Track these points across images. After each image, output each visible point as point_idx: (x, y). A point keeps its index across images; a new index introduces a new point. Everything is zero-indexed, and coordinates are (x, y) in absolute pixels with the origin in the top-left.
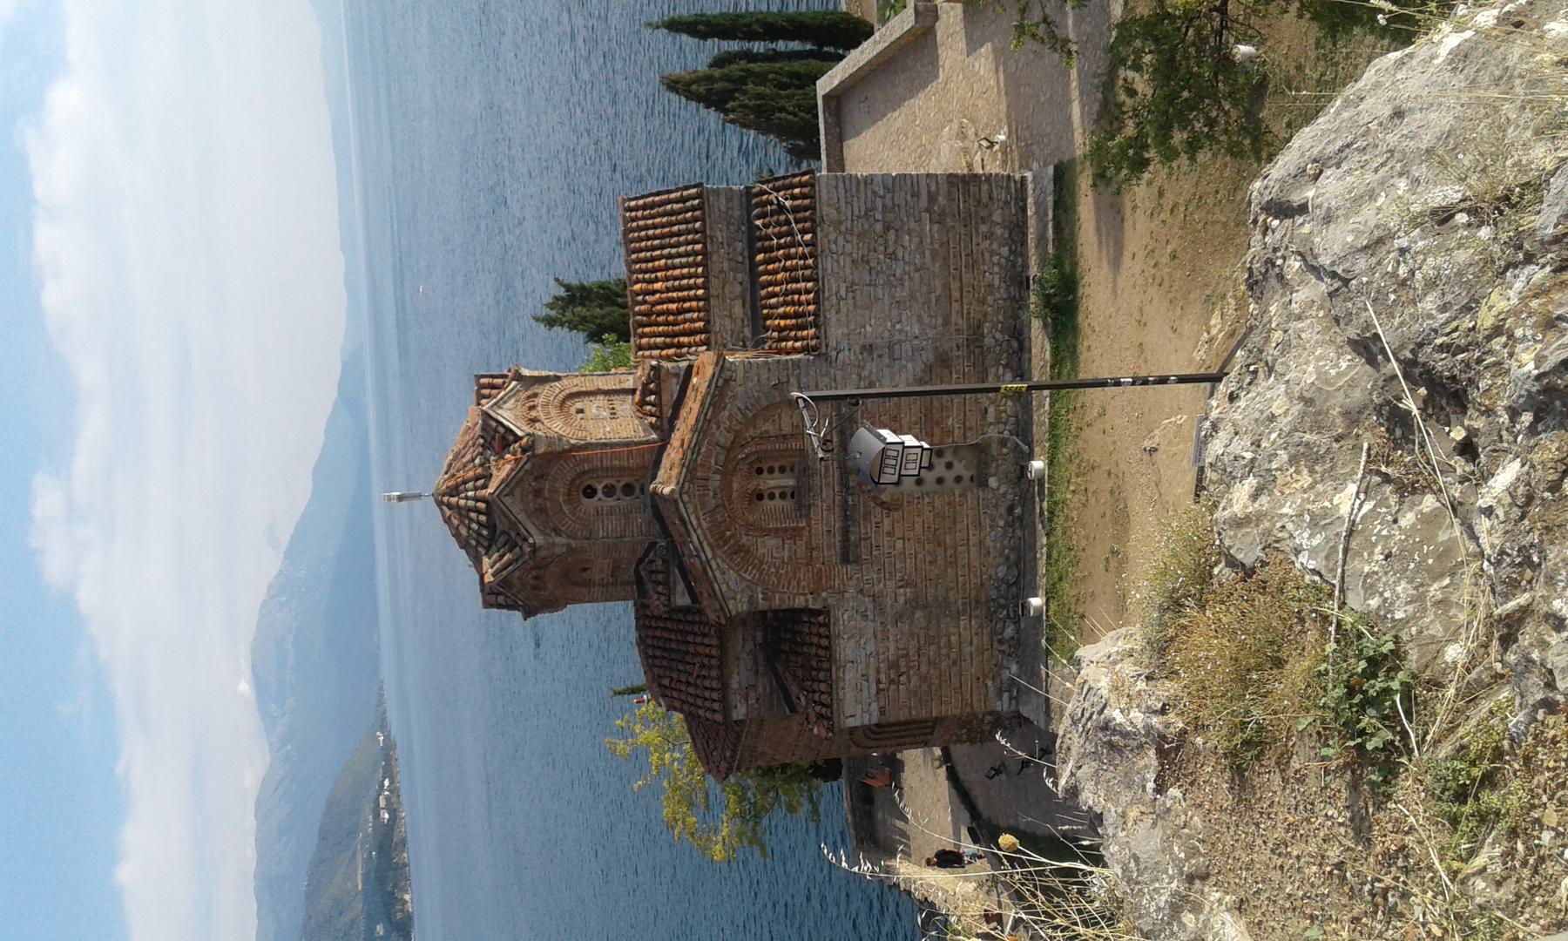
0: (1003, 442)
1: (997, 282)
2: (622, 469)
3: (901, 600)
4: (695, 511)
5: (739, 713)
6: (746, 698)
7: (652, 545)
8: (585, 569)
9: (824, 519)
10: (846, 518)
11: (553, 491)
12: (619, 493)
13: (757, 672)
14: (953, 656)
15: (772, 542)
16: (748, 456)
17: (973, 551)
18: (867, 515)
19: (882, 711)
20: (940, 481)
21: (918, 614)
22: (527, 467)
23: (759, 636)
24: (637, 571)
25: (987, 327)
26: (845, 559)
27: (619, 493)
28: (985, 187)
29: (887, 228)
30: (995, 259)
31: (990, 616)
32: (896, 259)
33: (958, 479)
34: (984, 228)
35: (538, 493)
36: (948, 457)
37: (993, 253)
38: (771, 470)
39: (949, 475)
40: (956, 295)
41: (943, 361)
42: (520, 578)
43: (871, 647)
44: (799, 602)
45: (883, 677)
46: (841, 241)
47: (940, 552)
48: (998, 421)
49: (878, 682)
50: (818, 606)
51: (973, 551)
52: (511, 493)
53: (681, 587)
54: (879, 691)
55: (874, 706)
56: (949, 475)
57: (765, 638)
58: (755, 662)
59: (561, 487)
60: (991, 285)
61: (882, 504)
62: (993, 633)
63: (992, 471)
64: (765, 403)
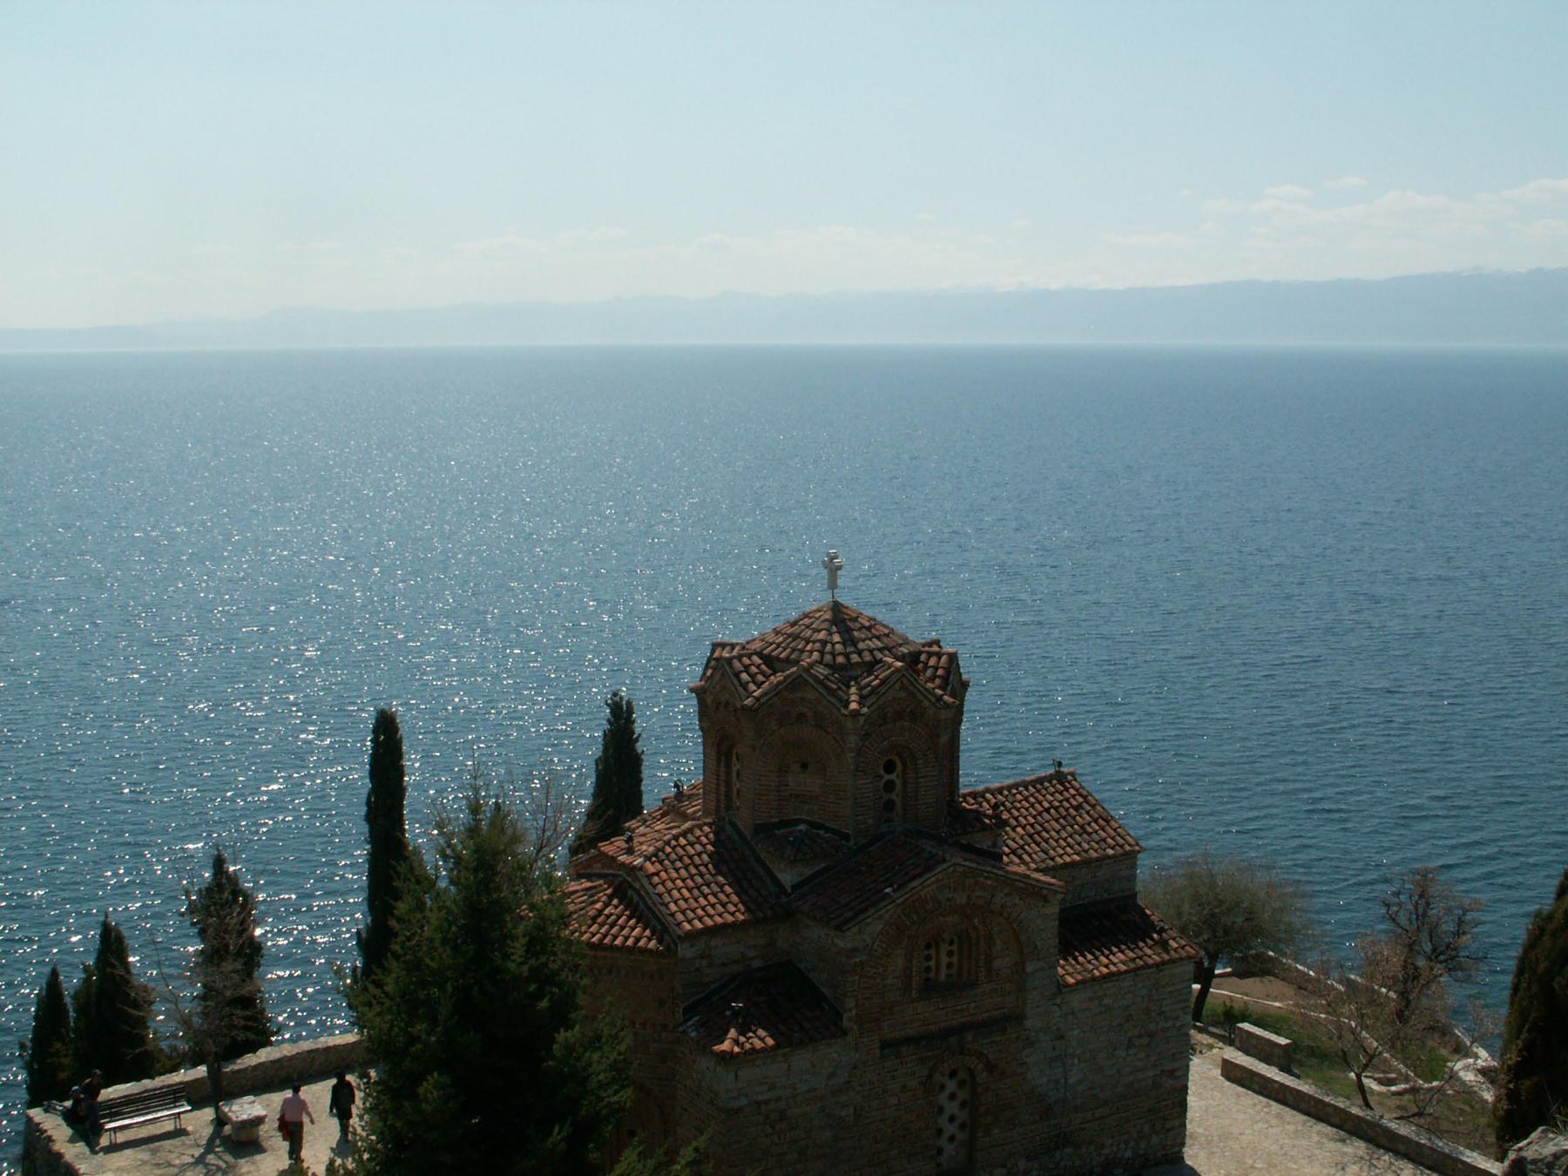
1: (1106, 1151)
3: (844, 1113)
4: (938, 880)
6: (702, 957)
7: (846, 837)
8: (804, 766)
13: (724, 965)
15: (900, 962)
16: (976, 928)
22: (926, 703)
23: (757, 964)
24: (797, 822)
25: (1069, 1150)
26: (885, 1045)
28: (1177, 1123)
29: (1150, 1035)
30: (1123, 1146)
32: (1128, 1048)
33: (940, 1151)
34: (1147, 1128)
36: (960, 1136)
37: (1127, 1143)
38: (950, 953)
39: (943, 1142)
40: (1098, 1113)
42: (802, 699)
46: (1145, 991)
49: (767, 1102)
50: (845, 1024)
52: (903, 688)
53: (808, 872)
54: (758, 1103)
55: (743, 1102)
56: (943, 1142)
57: (759, 969)
58: (735, 962)
60: (1103, 1146)
61: (930, 1076)
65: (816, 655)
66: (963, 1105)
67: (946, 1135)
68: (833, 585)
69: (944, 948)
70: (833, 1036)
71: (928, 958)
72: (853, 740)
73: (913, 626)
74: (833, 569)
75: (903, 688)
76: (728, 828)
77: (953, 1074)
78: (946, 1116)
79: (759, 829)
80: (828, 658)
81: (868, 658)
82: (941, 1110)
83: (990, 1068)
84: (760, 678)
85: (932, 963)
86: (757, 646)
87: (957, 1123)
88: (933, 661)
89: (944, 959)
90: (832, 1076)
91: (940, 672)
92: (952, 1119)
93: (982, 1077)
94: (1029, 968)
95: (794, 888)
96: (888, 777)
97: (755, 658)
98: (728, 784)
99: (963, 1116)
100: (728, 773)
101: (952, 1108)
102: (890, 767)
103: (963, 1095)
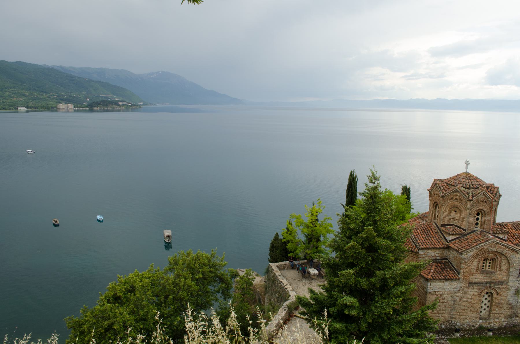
0: (489, 324)
2: (484, 223)
3: (457, 298)
5: (421, 252)
7: (465, 230)
8: (456, 211)
9: (479, 277)
10: (480, 283)
11: (482, 206)
12: (476, 221)
14: (440, 312)
15: (476, 263)
17: (464, 317)
18: (479, 289)
19: (430, 293)
20: (482, 307)
21: (452, 302)
23: (438, 258)
25: (517, 318)
26: (470, 283)
27: (476, 221)
31: (448, 322)
33: (481, 312)
35: (482, 201)
36: (487, 309)
38: (490, 263)
39: (482, 310)
41: (512, 308)
43: (447, 290)
44: (462, 271)
45: (439, 293)
47: (466, 308)
48: (494, 322)
50: (460, 276)
51: (464, 317)
53: (454, 237)
54: (435, 292)
56: (482, 310)
58: (433, 257)
59: (482, 208)
61: (481, 293)
62: (444, 322)
63: (484, 321)
64: (510, 262)
65: (462, 185)
66: (489, 301)
67: (483, 308)
68: (467, 168)
69: (488, 261)
70: (456, 279)
71: (484, 263)
72: (469, 207)
73: (488, 180)
74: (467, 164)
75: (484, 195)
76: (434, 224)
77: (487, 293)
78: (484, 303)
79: (442, 225)
80: (464, 185)
81: (475, 187)
82: (483, 302)
83: (497, 293)
84: (446, 189)
85: (485, 265)
86: (446, 181)
87: (486, 306)
88: (493, 189)
89: (488, 264)
90: (455, 288)
91: (495, 192)
92: (485, 304)
93: (495, 295)
94: (511, 270)
95: (450, 241)
96: (477, 217)
97: (445, 184)
98: (435, 214)
99: (488, 304)
100: (435, 211)
101: (486, 302)
102: (478, 214)
103: (489, 299)
